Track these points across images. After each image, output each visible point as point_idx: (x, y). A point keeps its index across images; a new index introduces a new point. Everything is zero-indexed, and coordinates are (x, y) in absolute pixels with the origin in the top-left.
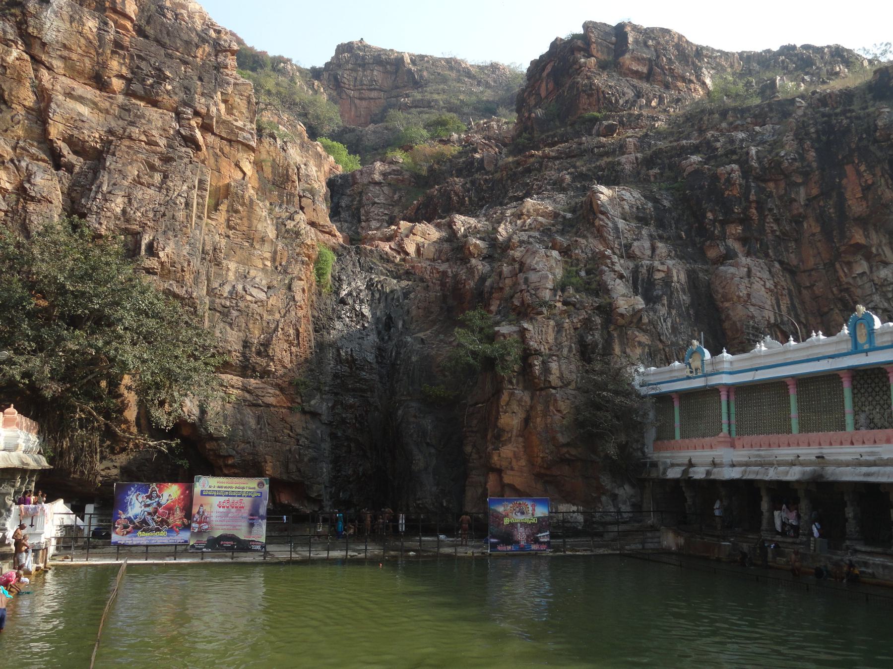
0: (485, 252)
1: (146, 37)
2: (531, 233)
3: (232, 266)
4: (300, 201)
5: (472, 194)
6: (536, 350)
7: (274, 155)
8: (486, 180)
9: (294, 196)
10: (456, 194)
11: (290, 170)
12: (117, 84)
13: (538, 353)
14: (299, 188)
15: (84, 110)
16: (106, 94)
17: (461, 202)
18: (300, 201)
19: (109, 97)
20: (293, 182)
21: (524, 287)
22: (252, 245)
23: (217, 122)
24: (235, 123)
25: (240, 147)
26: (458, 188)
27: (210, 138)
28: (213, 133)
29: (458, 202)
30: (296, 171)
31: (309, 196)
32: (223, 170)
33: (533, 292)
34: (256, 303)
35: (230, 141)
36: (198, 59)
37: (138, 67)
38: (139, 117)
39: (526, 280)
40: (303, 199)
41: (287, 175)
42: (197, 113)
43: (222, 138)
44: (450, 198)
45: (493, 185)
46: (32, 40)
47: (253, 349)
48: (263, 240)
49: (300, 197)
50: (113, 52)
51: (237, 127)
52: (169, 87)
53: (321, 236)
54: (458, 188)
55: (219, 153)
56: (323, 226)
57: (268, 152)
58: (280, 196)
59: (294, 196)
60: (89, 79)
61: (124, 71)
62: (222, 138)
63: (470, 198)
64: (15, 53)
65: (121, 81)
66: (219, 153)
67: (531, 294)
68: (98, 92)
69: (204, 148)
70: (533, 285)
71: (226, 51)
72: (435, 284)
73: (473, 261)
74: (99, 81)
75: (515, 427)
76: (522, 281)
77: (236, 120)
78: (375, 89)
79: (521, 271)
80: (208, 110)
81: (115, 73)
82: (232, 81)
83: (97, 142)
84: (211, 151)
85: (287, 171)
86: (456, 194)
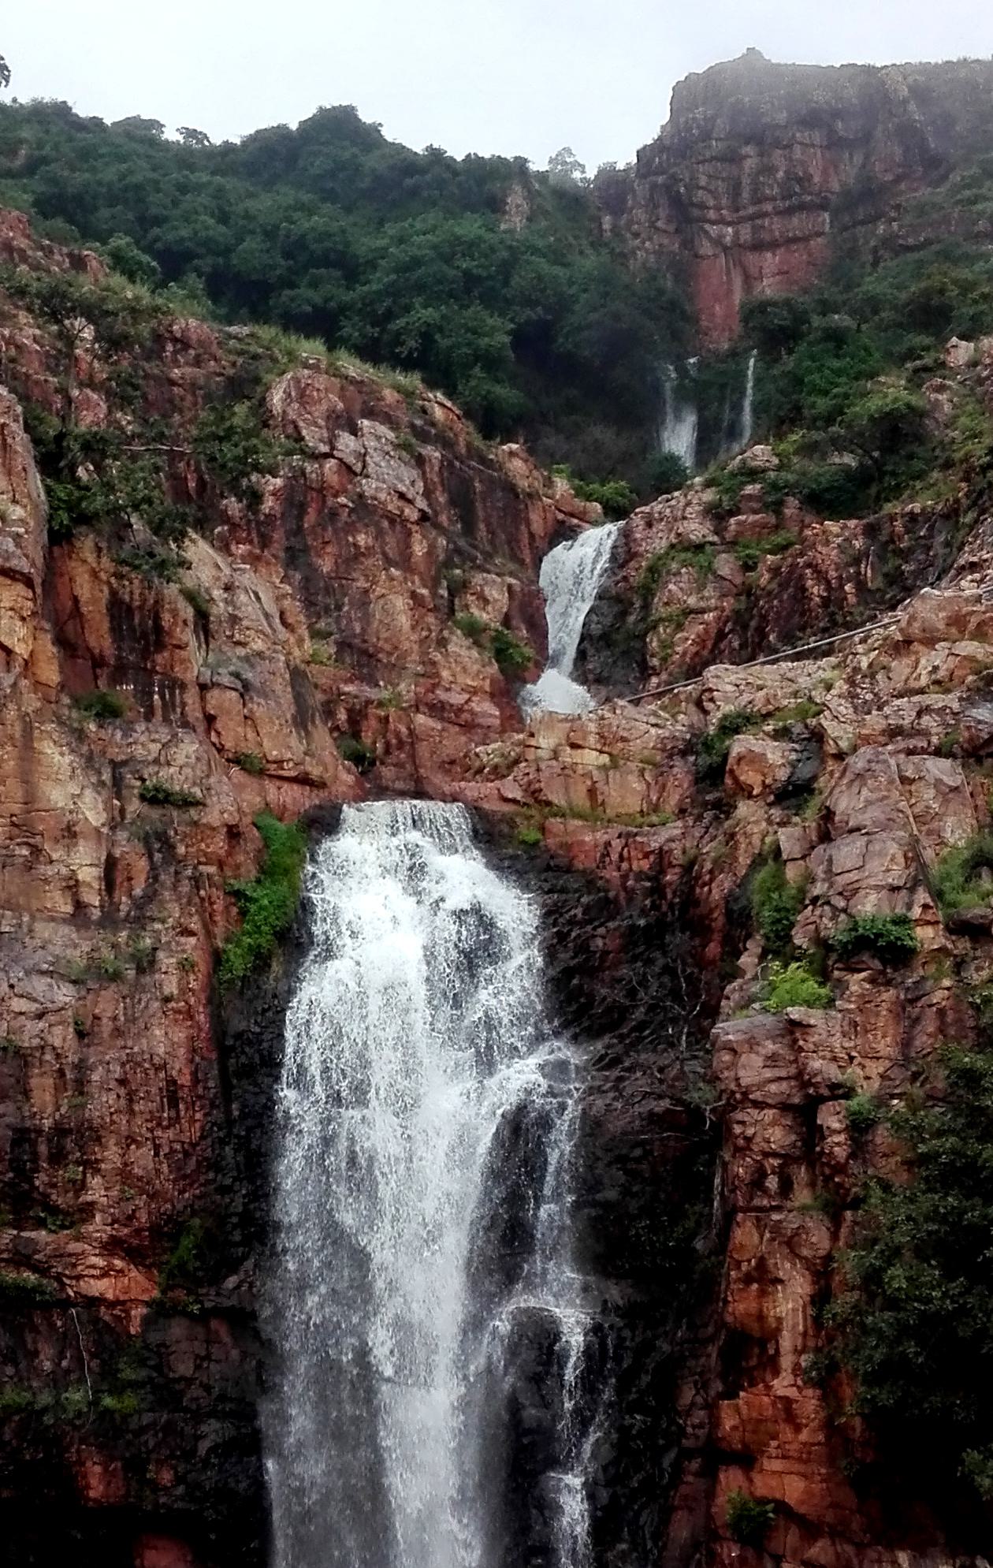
0: (783, 774)
2: (936, 700)
4: (203, 699)
6: (839, 1086)
9: (183, 686)
10: (820, 575)
11: (166, 619)
13: (841, 1091)
14: (195, 661)
17: (833, 600)
18: (203, 699)
21: (818, 889)
22: (36, 850)
26: (829, 555)
29: (826, 602)
33: (842, 904)
34: (40, 1016)
39: (830, 861)
41: (158, 629)
44: (804, 589)
47: (43, 1149)
48: (70, 834)
49: (203, 688)
54: (829, 555)
56: (279, 763)
63: (861, 585)
67: (834, 908)
70: (841, 880)
72: (630, 894)
75: (787, 1325)
76: (820, 872)
78: (802, 207)
79: (825, 837)
85: (157, 618)
86: (820, 575)
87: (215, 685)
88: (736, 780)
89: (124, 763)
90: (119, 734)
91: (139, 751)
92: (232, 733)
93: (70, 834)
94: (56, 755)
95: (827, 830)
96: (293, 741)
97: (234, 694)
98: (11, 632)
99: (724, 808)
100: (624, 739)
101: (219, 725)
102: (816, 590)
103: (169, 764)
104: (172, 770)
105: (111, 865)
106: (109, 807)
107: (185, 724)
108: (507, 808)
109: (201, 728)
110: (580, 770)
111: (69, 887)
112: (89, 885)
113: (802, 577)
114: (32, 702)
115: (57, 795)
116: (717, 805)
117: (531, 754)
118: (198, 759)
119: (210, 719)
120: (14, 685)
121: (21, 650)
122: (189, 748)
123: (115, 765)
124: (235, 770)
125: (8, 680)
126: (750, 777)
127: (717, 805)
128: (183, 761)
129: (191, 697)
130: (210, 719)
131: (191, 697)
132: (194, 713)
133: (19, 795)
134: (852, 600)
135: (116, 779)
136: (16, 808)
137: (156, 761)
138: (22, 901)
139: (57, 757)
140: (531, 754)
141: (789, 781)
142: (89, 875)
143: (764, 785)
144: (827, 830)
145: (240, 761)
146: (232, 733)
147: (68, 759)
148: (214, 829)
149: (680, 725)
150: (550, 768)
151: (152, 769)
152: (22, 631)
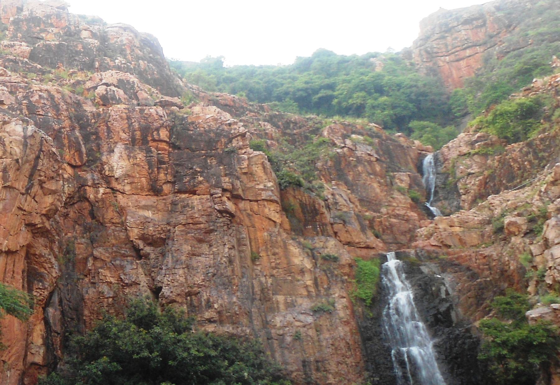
0: (524, 228)
1: (179, 148)
3: (280, 298)
5: (530, 156)
7: (300, 197)
8: (542, 140)
10: (515, 160)
12: (167, 188)
15: (149, 214)
16: (161, 198)
19: (163, 199)
20: (323, 213)
23: (243, 190)
24: (257, 187)
25: (266, 203)
27: (242, 205)
28: (243, 199)
30: (323, 203)
31: (338, 221)
32: (257, 225)
35: (257, 201)
36: (219, 150)
37: (177, 172)
38: (184, 207)
40: (335, 226)
42: (224, 190)
43: (251, 201)
44: (511, 166)
45: (550, 142)
46: (109, 178)
50: (158, 169)
51: (259, 189)
52: (201, 179)
53: (359, 252)
55: (251, 213)
57: (294, 197)
58: (315, 228)
59: (326, 225)
60: (149, 191)
61: (169, 178)
62: (251, 201)
63: (530, 162)
64: (102, 190)
65: (169, 185)
66: (251, 213)
68: (154, 199)
69: (238, 214)
71: (236, 137)
73: (513, 239)
74: (155, 190)
77: (258, 184)
80: (233, 185)
81: (163, 181)
82: (246, 156)
83: (161, 234)
84: (244, 213)
87: (335, 223)
88: (508, 230)
89: (314, 249)
90: (310, 241)
91: (317, 245)
92: (344, 236)
93: (302, 272)
94: (294, 250)
95: (547, 245)
96: (362, 236)
97: (341, 225)
98: (275, 217)
99: (506, 240)
100: (467, 222)
101: (339, 234)
102: (516, 166)
103: (327, 248)
104: (328, 250)
105: (315, 280)
106: (312, 262)
107: (329, 236)
108: (433, 248)
109: (334, 236)
110: (455, 234)
111: (305, 287)
112: (310, 286)
113: (509, 162)
114: (285, 235)
115: (297, 261)
116: (504, 239)
117: (437, 231)
118: (335, 246)
119: (336, 233)
120: (279, 231)
121: (278, 221)
122: (332, 242)
123: (311, 250)
124: (346, 246)
125: (276, 230)
126: (513, 229)
127: (504, 239)
128: (331, 246)
129: (329, 228)
130: (336, 233)
131: (329, 228)
132: (331, 232)
133: (285, 262)
134: (528, 167)
135: (312, 254)
136: (285, 266)
137: (323, 247)
138: (292, 292)
139: (295, 250)
140: (437, 231)
141: (527, 229)
142: (309, 283)
143: (519, 231)
144: (547, 245)
145: (349, 244)
146: (344, 236)
147: (298, 250)
148: (344, 265)
149: (485, 215)
150: (444, 234)
151: (322, 250)
152: (277, 216)
